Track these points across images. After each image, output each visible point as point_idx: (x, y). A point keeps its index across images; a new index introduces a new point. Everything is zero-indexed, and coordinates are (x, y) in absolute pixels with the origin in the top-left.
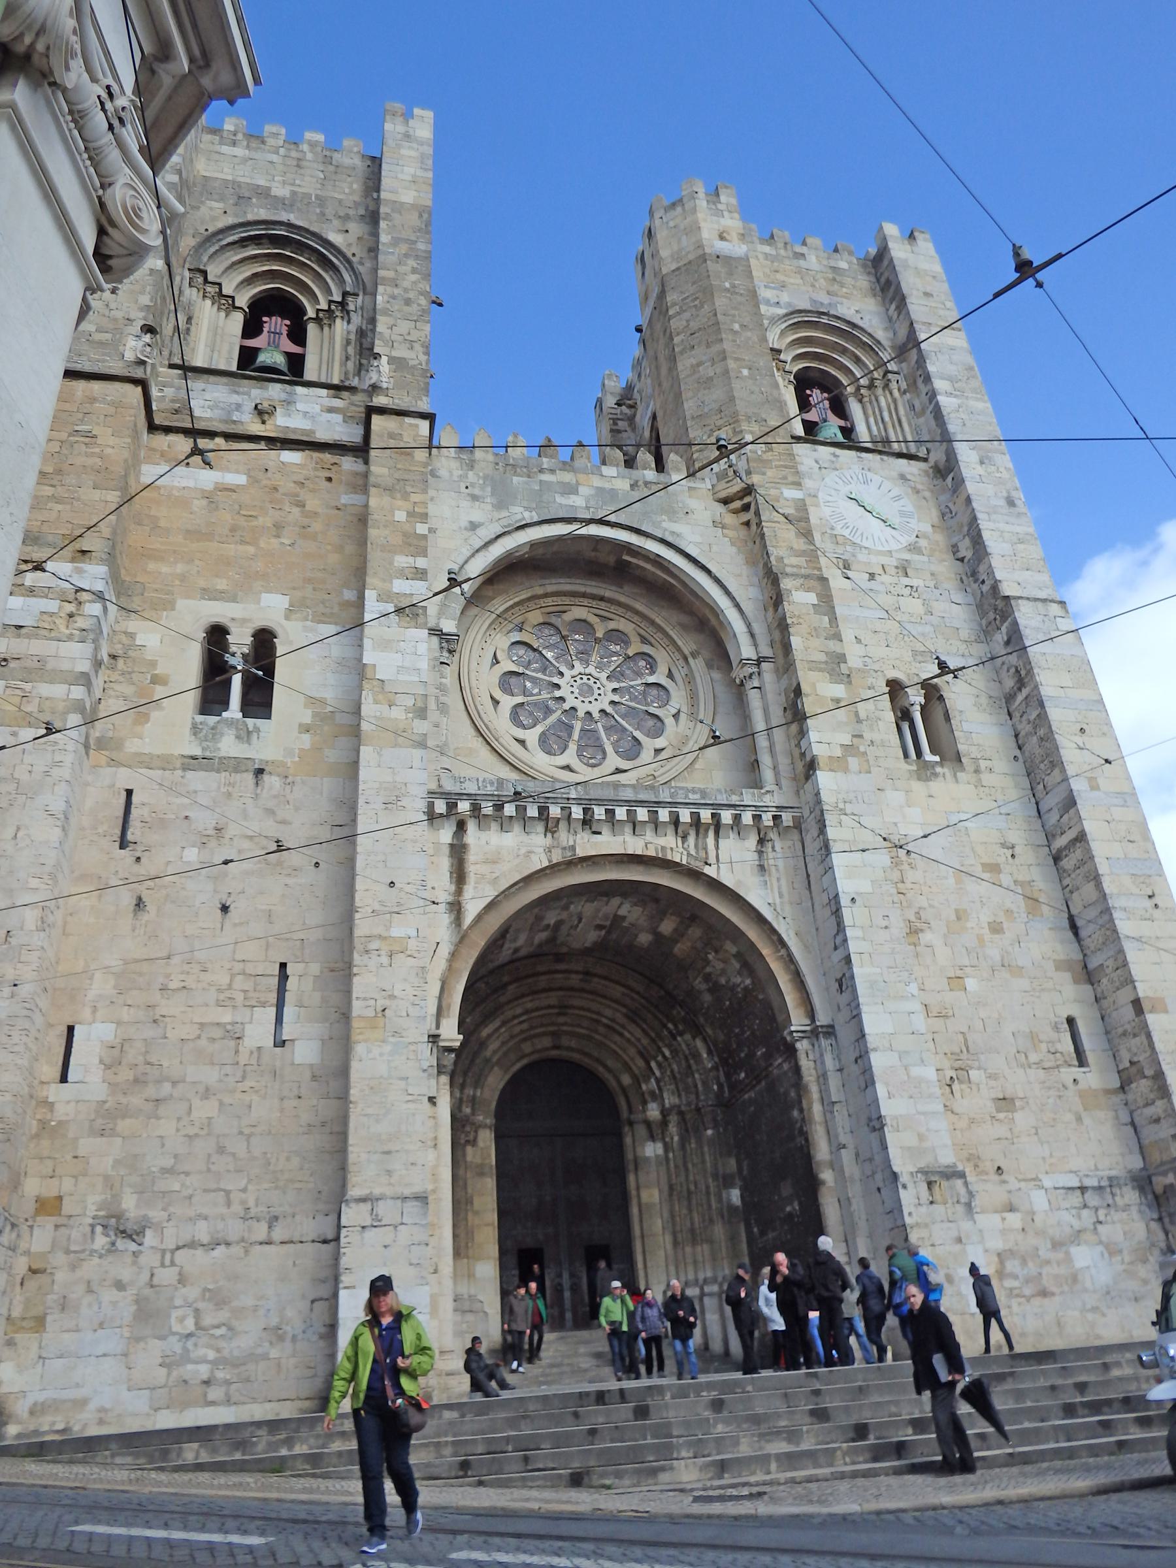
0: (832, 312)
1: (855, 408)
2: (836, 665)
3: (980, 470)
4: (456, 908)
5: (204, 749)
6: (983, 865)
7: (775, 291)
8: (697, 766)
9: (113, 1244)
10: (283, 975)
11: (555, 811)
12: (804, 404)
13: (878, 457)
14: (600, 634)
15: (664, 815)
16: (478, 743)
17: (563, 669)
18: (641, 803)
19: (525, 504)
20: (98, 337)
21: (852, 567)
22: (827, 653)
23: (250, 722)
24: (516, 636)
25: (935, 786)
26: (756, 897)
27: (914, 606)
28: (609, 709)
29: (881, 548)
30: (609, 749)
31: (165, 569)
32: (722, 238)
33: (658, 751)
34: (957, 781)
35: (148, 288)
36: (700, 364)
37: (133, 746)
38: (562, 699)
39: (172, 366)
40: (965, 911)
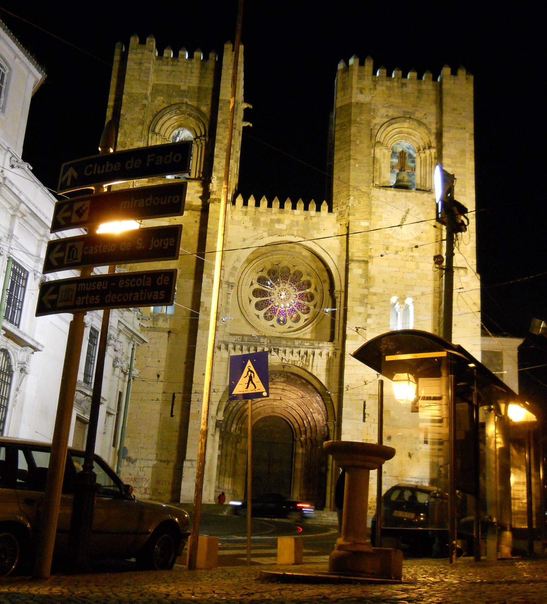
0: (412, 117)
2: (363, 300)
5: (153, 324)
9: (129, 464)
10: (174, 397)
14: (292, 272)
15: (296, 351)
18: (286, 347)
19: (264, 229)
21: (389, 249)
22: (361, 295)
24: (260, 274)
27: (411, 265)
30: (288, 318)
32: (361, 92)
33: (306, 320)
36: (341, 159)
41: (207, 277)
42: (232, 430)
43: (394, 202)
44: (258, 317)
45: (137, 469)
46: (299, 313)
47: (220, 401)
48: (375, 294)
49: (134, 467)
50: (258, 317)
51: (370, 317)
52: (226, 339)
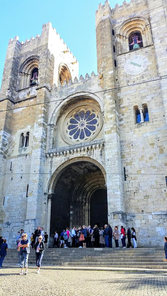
0: (134, 17)
1: (143, 36)
3: (160, 45)
4: (51, 171)
6: (150, 144)
7: (121, 19)
8: (99, 135)
11: (65, 152)
12: (130, 41)
13: (140, 50)
16: (62, 141)
17: (78, 122)
20: (3, 93)
23: (26, 147)
24: (71, 118)
25: (141, 128)
26: (99, 161)
28: (86, 127)
29: (138, 74)
30: (85, 135)
31: (16, 126)
32: (104, 16)
34: (147, 126)
35: (9, 82)
37: (12, 155)
38: (78, 128)
39: (17, 92)
40: (144, 156)
41: (36, 124)
42: (78, 200)
43: (130, 58)
44: (71, 139)
45: (11, 228)
46: (90, 131)
47: (50, 184)
48: (124, 107)
49: (10, 227)
50: (71, 139)
51: (123, 120)
52: (49, 152)
